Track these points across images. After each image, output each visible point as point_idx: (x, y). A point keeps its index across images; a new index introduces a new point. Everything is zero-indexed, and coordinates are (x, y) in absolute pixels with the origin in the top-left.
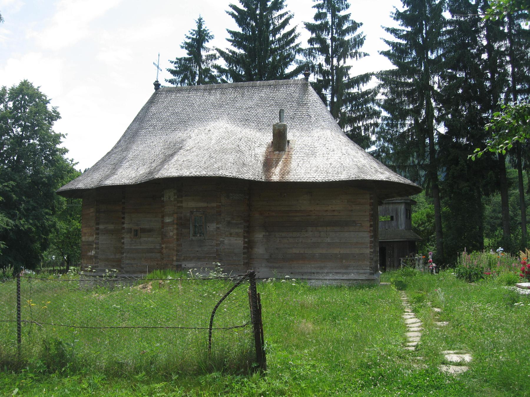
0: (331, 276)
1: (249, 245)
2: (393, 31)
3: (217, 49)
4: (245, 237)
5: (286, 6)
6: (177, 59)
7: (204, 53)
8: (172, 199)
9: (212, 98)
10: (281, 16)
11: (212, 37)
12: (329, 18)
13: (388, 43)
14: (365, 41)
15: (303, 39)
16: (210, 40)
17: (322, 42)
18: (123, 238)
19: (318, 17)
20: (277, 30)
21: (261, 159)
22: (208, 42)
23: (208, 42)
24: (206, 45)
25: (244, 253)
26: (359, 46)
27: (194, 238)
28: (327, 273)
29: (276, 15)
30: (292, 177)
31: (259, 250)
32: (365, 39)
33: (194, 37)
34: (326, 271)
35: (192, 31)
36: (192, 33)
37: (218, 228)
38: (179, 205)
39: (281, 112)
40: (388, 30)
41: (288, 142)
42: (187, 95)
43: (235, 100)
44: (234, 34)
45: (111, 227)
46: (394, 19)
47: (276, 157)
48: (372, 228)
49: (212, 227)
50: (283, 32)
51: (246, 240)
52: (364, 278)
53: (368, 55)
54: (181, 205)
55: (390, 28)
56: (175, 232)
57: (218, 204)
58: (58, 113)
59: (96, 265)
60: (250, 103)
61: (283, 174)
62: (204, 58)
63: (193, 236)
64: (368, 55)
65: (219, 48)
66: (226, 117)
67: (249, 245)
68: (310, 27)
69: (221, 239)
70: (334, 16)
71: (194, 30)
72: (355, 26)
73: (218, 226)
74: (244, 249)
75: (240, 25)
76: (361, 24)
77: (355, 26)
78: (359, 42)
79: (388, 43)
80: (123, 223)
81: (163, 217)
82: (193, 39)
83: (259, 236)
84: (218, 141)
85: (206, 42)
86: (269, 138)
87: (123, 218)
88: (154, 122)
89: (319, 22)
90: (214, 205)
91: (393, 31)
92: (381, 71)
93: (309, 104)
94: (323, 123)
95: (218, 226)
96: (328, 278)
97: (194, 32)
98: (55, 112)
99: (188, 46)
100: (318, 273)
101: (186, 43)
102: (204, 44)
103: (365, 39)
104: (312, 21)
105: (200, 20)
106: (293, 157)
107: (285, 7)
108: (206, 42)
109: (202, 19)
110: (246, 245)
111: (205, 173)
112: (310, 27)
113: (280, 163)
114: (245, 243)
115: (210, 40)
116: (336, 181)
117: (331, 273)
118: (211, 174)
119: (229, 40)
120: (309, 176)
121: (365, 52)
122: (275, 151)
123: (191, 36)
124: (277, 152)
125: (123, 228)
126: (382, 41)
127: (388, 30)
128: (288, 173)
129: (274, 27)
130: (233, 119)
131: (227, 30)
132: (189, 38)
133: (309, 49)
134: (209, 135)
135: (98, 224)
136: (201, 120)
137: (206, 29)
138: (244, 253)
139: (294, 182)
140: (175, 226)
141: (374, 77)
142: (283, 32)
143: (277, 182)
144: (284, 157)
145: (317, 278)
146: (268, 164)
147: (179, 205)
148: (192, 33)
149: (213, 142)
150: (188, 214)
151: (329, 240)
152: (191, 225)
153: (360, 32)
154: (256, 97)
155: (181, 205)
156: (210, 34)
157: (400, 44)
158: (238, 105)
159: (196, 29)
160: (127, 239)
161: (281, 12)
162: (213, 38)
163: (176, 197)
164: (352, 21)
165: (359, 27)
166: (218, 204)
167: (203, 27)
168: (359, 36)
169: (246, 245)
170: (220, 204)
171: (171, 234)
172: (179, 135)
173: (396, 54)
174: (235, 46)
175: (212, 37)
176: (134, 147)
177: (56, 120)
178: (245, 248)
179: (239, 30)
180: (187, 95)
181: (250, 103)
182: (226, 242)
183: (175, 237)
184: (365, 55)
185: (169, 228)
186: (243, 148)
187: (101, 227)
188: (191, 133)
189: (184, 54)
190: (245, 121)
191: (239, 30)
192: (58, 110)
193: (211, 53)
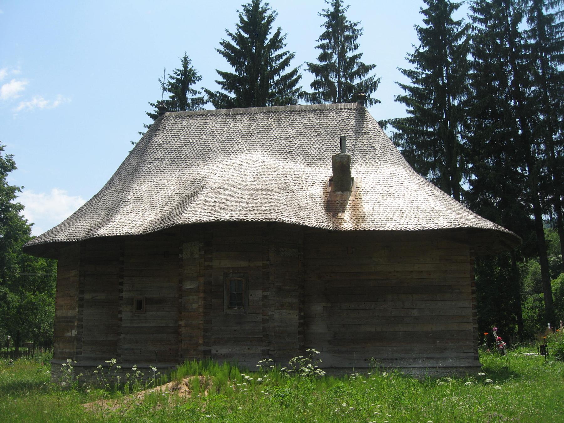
0: (420, 364)
1: (306, 321)
2: (410, 74)
3: (206, 91)
4: (300, 310)
5: (285, 45)
6: (158, 101)
7: (189, 97)
8: (197, 256)
9: (238, 125)
10: (279, 57)
11: (199, 78)
12: (335, 58)
13: (405, 87)
14: (379, 85)
15: (306, 81)
16: (197, 82)
17: (329, 84)
18: (120, 312)
19: (322, 58)
20: (276, 71)
21: (320, 201)
22: (195, 83)
23: (195, 83)
24: (192, 87)
25: (300, 333)
26: (371, 91)
27: (229, 312)
28: (415, 359)
29: (274, 55)
30: (370, 225)
31: (319, 328)
32: (379, 82)
33: (179, 77)
34: (414, 356)
35: (176, 71)
36: (176, 73)
37: (265, 297)
38: (207, 264)
39: (343, 140)
40: (404, 72)
41: (353, 178)
42: (203, 121)
43: (269, 127)
44: (225, 75)
45: (101, 296)
46: (410, 61)
47: (339, 198)
48: (475, 296)
49: (257, 295)
50: (283, 73)
51: (302, 314)
52: (467, 365)
53: (380, 102)
54: (210, 264)
55: (407, 69)
56: (201, 302)
57: (265, 262)
58: (13, 163)
59: (79, 350)
60: (291, 132)
61: (357, 221)
62: (190, 101)
63: (229, 308)
64: (380, 102)
65: (208, 89)
66: (259, 149)
67: (306, 321)
68: (313, 69)
69: (270, 313)
70: (342, 55)
71: (178, 70)
72: (365, 69)
73: (265, 294)
74: (299, 327)
75: (233, 64)
76: (374, 66)
77: (365, 69)
78: (373, 85)
79: (405, 87)
80: (121, 291)
81: (181, 281)
82: (177, 80)
83: (318, 308)
84: (257, 178)
85: (193, 84)
86: (326, 172)
87: (121, 284)
88: (161, 154)
89: (324, 63)
90: (260, 264)
91: (410, 74)
92: (396, 119)
93: (370, 133)
94: (392, 157)
95: (265, 294)
96: (417, 366)
97: (179, 72)
98: (9, 160)
99: (173, 88)
100: (402, 359)
101: (170, 84)
102: (190, 86)
103: (379, 82)
104: (317, 62)
105: (186, 58)
106: (363, 199)
107: (284, 46)
108: (193, 84)
109: (188, 57)
110: (302, 321)
111: (253, 217)
112: (313, 69)
113: (347, 206)
114: (301, 318)
115: (197, 82)
116: (433, 230)
117: (420, 358)
118: (260, 217)
119: (219, 82)
120: (393, 223)
121: (376, 98)
122: (336, 191)
123: (175, 76)
124: (340, 193)
125: (121, 298)
126: (397, 85)
127: (404, 72)
128: (363, 219)
129: (271, 68)
130: (273, 152)
131: (217, 71)
132: (173, 78)
133: (313, 94)
134: (241, 170)
135: (82, 292)
136: (226, 152)
137: (193, 69)
138: (300, 333)
139: (374, 232)
140: (202, 295)
141: (389, 125)
142: (283, 73)
143: (351, 231)
144: (351, 198)
145: (402, 366)
146: (333, 206)
147: (207, 264)
148: (176, 73)
149: (249, 178)
150: (222, 277)
151: (415, 313)
152: (225, 292)
153: (373, 75)
154: (298, 126)
155: (210, 264)
156: (198, 75)
157: (418, 88)
158: (274, 133)
159: (182, 68)
160: (126, 313)
161: (279, 52)
162: (200, 79)
163: (203, 253)
164: (361, 63)
165: (371, 69)
166: (265, 262)
167: (190, 66)
168: (371, 79)
169: (302, 321)
170: (268, 262)
171: (195, 306)
172: (200, 171)
173: (415, 98)
174: (226, 89)
175: (199, 78)
176: (136, 186)
177: (10, 171)
178: (301, 325)
179: (232, 70)
180: (203, 121)
181: (291, 132)
182: (277, 316)
183: (201, 310)
184: (377, 101)
185: (191, 297)
186: (292, 186)
187: (87, 296)
188: (214, 168)
189: (167, 96)
190: (288, 153)
191: (232, 70)
192: (14, 159)
193: (198, 96)
